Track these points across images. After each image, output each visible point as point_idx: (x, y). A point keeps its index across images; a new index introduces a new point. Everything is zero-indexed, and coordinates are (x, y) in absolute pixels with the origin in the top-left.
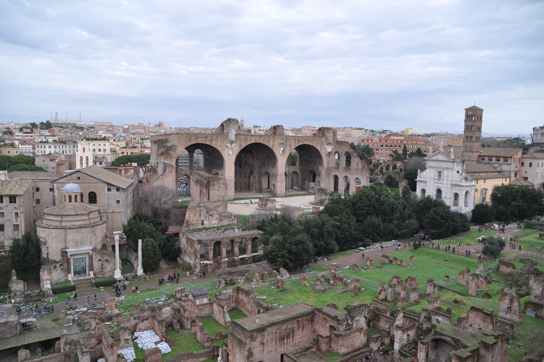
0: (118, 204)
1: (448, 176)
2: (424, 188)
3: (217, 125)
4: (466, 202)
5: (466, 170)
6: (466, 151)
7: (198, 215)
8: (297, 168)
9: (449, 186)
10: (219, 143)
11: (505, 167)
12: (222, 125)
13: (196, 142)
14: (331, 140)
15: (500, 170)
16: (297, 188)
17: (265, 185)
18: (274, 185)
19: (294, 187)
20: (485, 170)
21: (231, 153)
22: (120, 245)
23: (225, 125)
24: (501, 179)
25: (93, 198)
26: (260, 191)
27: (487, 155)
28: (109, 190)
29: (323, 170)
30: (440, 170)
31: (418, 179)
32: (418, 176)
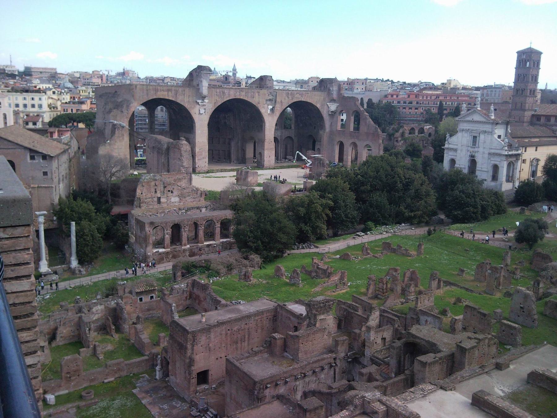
0: (46, 177)
1: (485, 142)
2: (453, 157)
5: (511, 134)
6: (515, 109)
7: (153, 190)
8: (292, 133)
9: (486, 156)
12: (191, 74)
14: (335, 96)
18: (260, 154)
20: (539, 135)
21: (202, 111)
22: (45, 231)
23: (195, 74)
26: (242, 160)
27: (544, 114)
28: (32, 158)
29: (325, 135)
31: (446, 146)
32: (446, 142)
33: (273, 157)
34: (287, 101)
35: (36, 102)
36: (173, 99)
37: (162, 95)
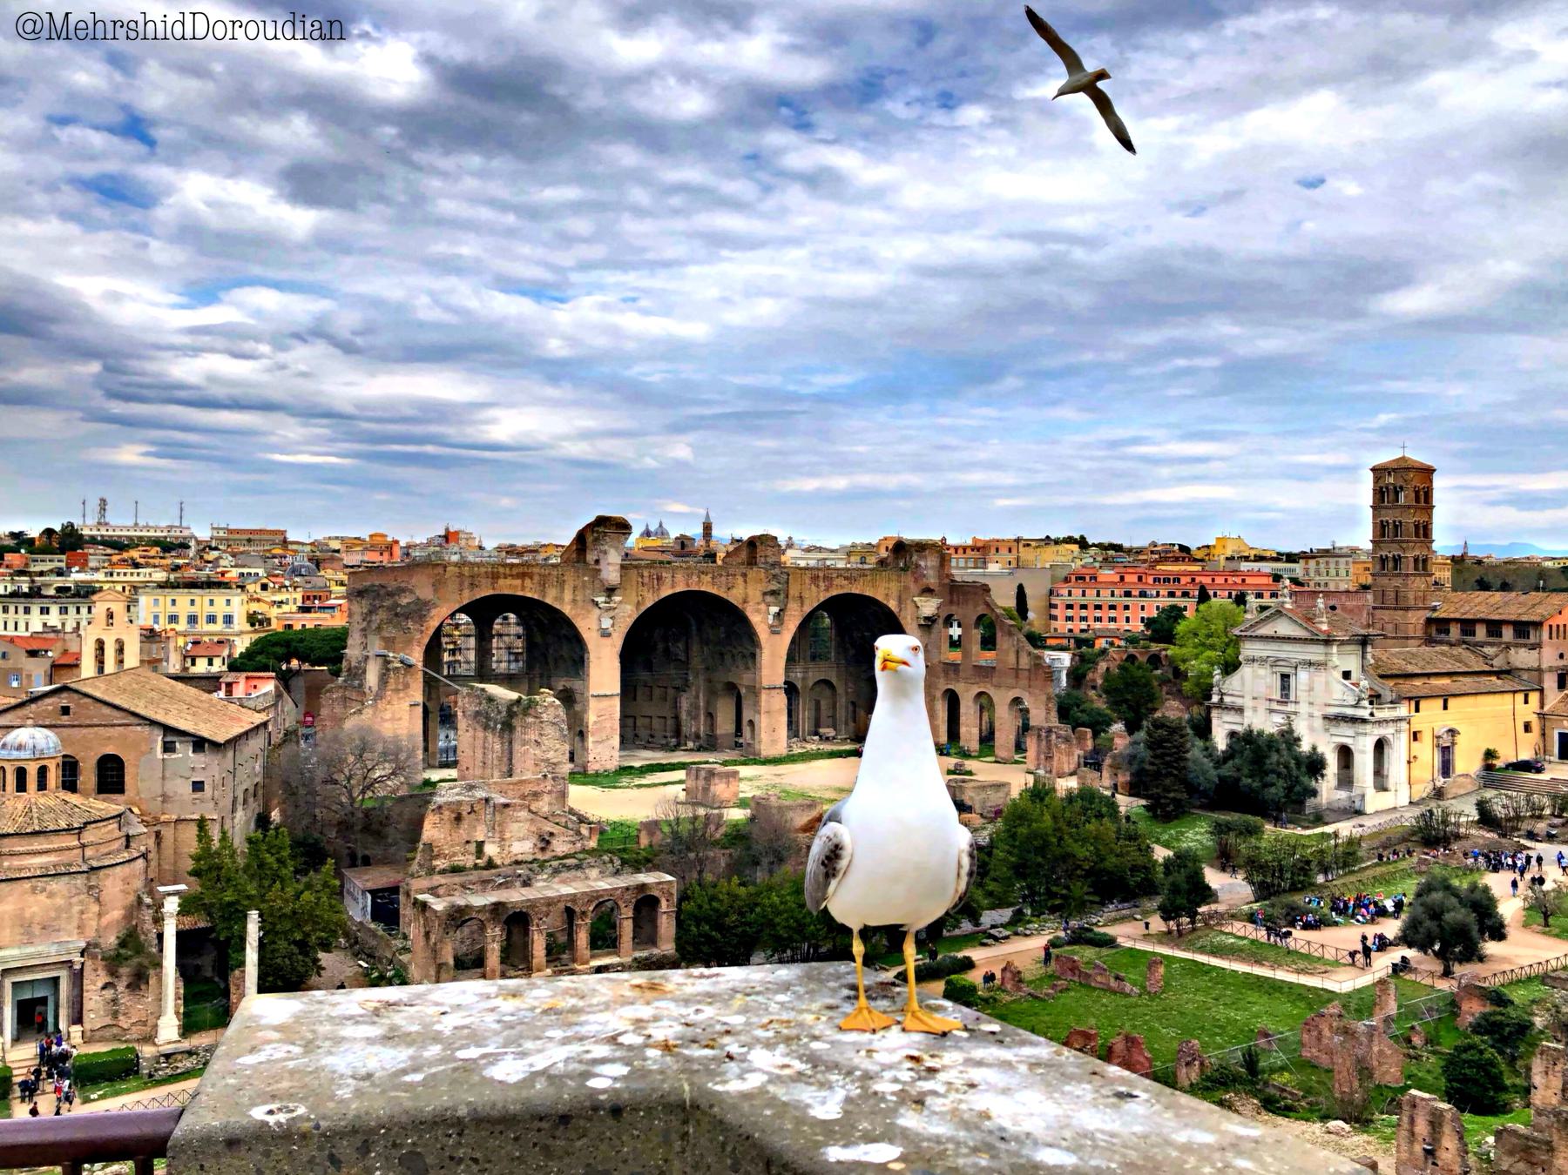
0: (198, 795)
3: (566, 538)
4: (1379, 772)
9: (1319, 723)
10: (568, 596)
11: (1522, 657)
13: (491, 592)
14: (932, 580)
15: (1506, 668)
16: (830, 732)
17: (725, 726)
18: (751, 723)
19: (822, 730)
22: (180, 935)
24: (1509, 697)
25: (111, 776)
27: (1457, 615)
28: (168, 748)
30: (1286, 670)
33: (783, 731)
34: (816, 596)
35: (220, 609)
36: (536, 597)
37: (507, 587)
